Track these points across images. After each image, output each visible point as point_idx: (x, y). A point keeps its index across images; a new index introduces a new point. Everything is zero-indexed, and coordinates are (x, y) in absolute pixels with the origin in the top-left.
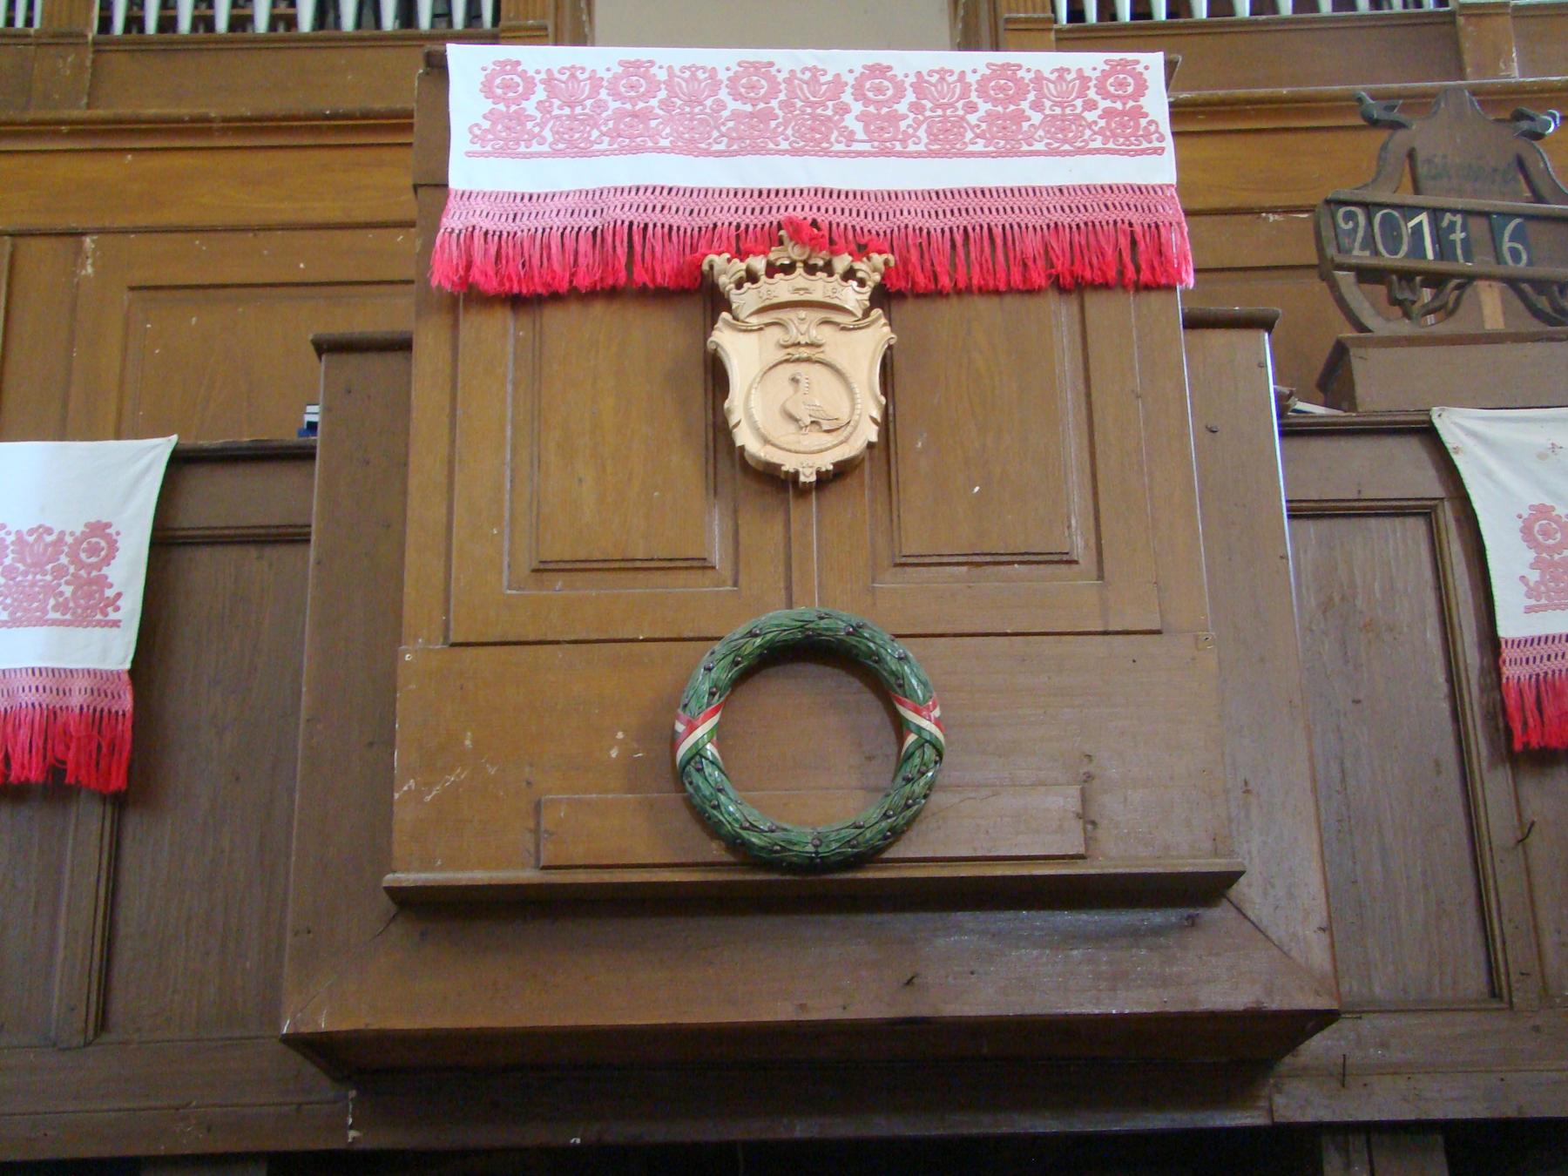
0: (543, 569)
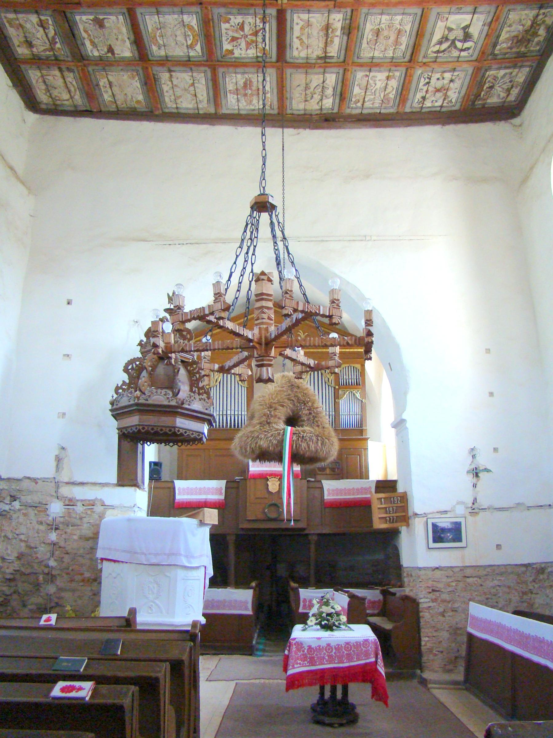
0: (257, 498)
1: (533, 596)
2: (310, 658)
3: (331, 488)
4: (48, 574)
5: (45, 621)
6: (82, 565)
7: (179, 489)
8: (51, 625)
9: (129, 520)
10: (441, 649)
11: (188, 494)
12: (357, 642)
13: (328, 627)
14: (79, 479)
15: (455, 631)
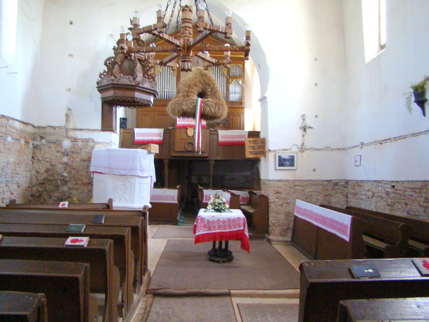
1: (331, 197)
2: (208, 227)
3: (223, 135)
4: (63, 180)
5: (62, 205)
6: (82, 175)
7: (137, 133)
8: (65, 208)
9: (108, 150)
10: (279, 224)
11: (142, 136)
12: (234, 219)
13: (219, 211)
14: (79, 127)
15: (288, 214)
